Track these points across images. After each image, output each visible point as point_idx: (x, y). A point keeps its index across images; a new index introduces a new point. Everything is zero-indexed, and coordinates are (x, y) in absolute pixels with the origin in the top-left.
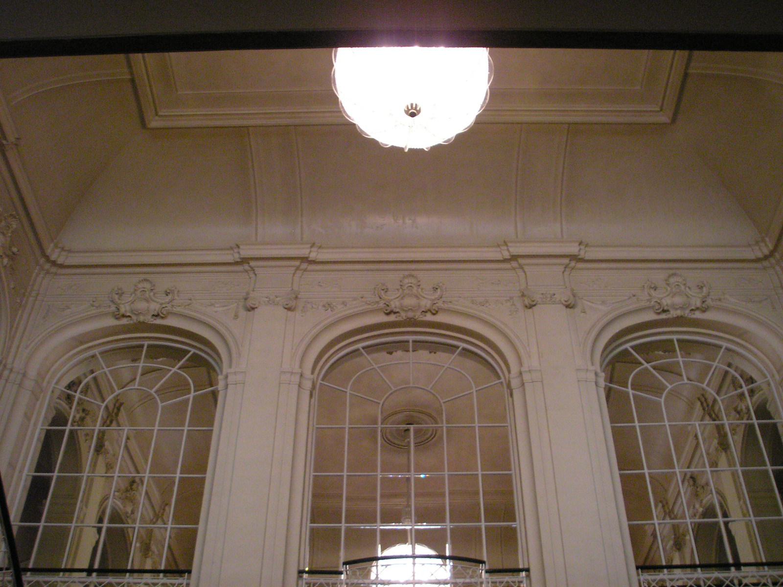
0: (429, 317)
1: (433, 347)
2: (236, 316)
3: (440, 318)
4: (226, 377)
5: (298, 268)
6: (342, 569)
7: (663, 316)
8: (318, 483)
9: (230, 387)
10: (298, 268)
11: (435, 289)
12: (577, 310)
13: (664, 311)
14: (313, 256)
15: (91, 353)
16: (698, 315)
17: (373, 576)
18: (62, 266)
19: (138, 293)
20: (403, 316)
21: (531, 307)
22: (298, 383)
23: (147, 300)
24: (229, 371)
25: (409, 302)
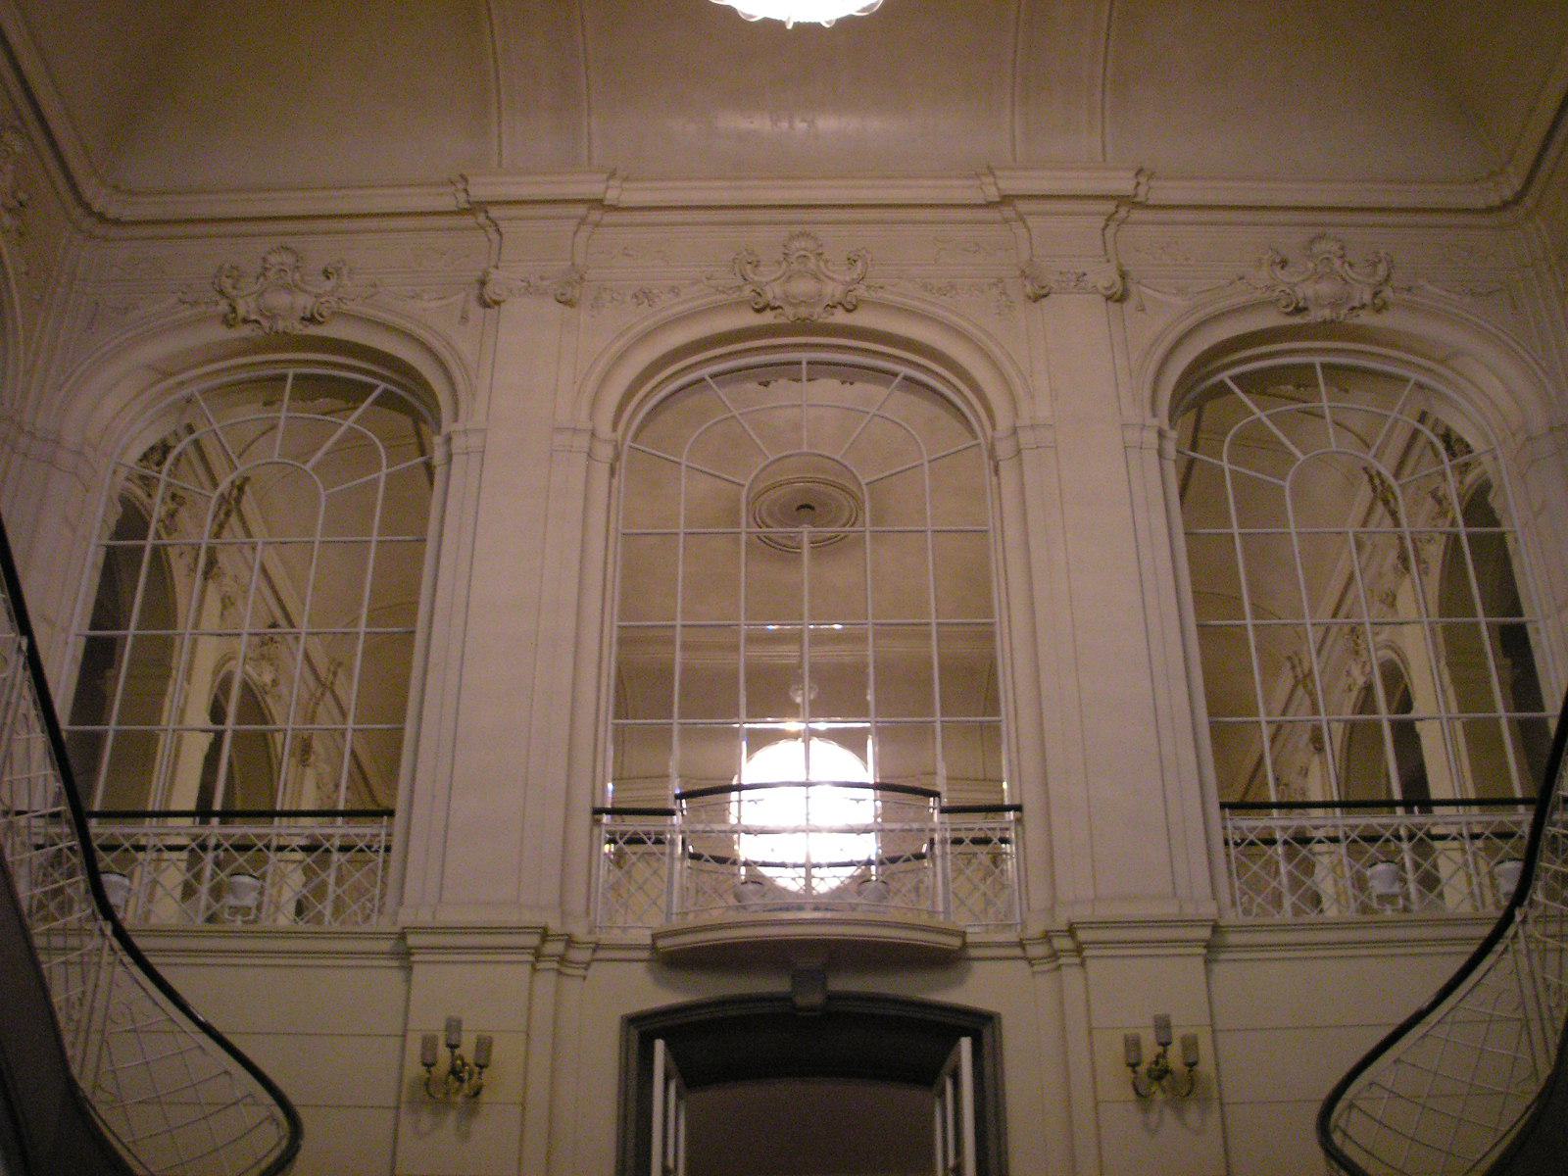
0: (840, 317)
1: (849, 373)
2: (464, 319)
3: (862, 319)
4: (449, 439)
5: (583, 221)
6: (671, 805)
7: (1297, 320)
8: (628, 640)
9: (455, 459)
10: (583, 221)
11: (852, 261)
12: (1131, 304)
13: (1299, 310)
14: (611, 196)
15: (185, 392)
16: (1366, 318)
17: (733, 820)
18: (117, 222)
19: (271, 274)
20: (789, 314)
21: (1036, 299)
22: (587, 450)
23: (289, 289)
24: (454, 427)
25: (802, 287)
